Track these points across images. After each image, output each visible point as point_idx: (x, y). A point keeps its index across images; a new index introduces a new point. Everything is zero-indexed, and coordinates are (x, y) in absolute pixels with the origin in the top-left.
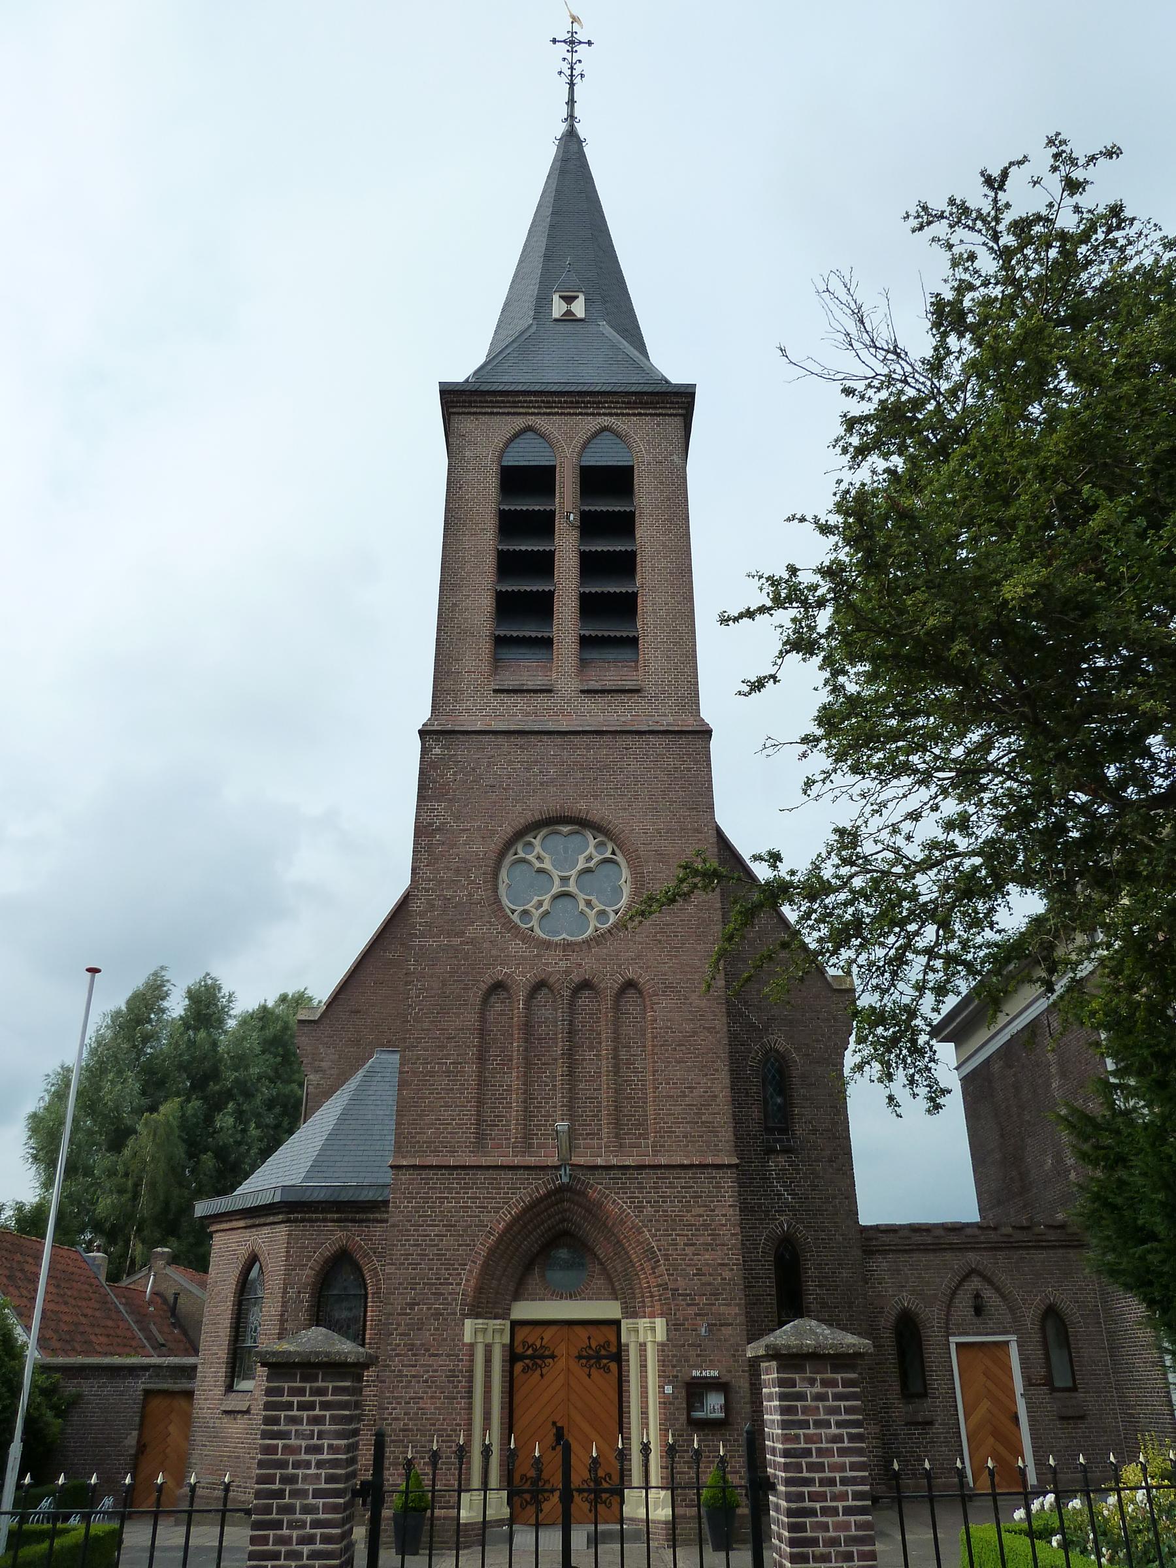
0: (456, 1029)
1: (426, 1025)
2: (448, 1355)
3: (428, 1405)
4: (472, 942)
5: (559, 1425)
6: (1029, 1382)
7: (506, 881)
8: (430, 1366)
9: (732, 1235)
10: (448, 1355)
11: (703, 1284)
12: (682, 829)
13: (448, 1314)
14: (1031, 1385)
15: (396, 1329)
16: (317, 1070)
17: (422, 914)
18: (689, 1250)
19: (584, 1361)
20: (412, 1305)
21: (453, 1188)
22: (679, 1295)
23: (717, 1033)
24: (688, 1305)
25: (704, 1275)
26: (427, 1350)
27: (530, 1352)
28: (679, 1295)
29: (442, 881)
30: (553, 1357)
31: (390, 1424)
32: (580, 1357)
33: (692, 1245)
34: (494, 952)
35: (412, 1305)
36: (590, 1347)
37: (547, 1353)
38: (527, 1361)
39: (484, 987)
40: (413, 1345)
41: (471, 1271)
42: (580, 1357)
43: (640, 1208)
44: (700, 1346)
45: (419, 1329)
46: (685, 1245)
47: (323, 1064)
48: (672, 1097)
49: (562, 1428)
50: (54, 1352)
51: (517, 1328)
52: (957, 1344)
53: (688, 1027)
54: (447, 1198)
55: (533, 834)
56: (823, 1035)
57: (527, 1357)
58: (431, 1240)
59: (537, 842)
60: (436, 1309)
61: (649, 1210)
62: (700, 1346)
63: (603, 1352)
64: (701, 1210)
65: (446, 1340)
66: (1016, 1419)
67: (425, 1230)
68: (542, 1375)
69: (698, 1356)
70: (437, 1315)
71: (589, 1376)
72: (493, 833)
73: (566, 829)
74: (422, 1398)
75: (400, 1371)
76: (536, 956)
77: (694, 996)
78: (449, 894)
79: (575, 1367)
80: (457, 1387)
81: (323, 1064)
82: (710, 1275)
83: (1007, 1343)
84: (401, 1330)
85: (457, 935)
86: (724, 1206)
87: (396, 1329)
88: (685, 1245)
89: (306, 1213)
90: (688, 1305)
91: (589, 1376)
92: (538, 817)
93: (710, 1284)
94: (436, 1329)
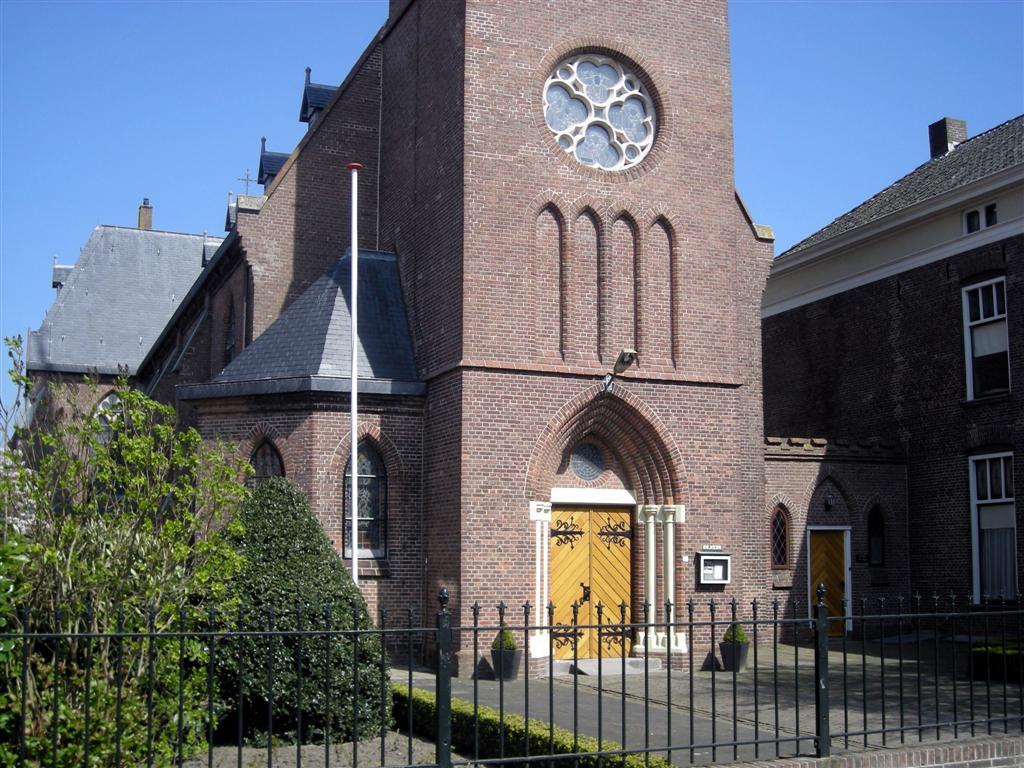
0: (513, 244)
1: (486, 237)
2: (518, 530)
3: (503, 570)
4: (524, 160)
5: (586, 585)
6: (856, 558)
7: (547, 104)
8: (503, 538)
9: (735, 441)
10: (518, 530)
11: (712, 479)
12: (704, 79)
13: (516, 496)
14: (858, 561)
15: (473, 508)
16: (262, 262)
17: (478, 127)
18: (703, 452)
19: (605, 537)
20: (486, 488)
21: (515, 390)
22: (695, 487)
23: (728, 271)
24: (701, 495)
25: (713, 472)
26: (500, 525)
27: (562, 529)
28: (695, 487)
29: (493, 95)
30: (581, 533)
31: (472, 585)
32: (602, 534)
33: (706, 448)
34: (544, 174)
35: (486, 488)
36: (609, 526)
37: (576, 530)
38: (561, 536)
39: (536, 206)
40: (488, 521)
41: (533, 462)
42: (602, 534)
43: (667, 416)
44: (708, 526)
45: (492, 508)
46: (700, 447)
47: (267, 256)
48: (692, 323)
49: (589, 588)
50: (362, 516)
51: (982, 509)
52: (812, 531)
53: (706, 264)
54: (511, 398)
55: (570, 60)
56: (747, 277)
57: (560, 533)
58: (499, 434)
59: (574, 67)
60: (505, 492)
61: (673, 418)
62: (708, 526)
63: (619, 530)
64: (712, 421)
65: (514, 517)
66: (842, 584)
67: (494, 425)
68: (572, 547)
69: (707, 534)
70: (507, 496)
71: (609, 548)
72: (539, 53)
73: (601, 60)
74: (497, 564)
75: (478, 542)
76: (581, 182)
77: (711, 236)
78: (501, 109)
79: (596, 539)
80: (525, 555)
81: (267, 256)
82: (718, 472)
83: (842, 531)
84: (479, 507)
85: (510, 152)
86: (729, 418)
87: (473, 508)
88: (700, 447)
89: (333, 402)
90: (701, 495)
91: (609, 548)
92: (580, 44)
93: (718, 480)
94: (507, 509)
